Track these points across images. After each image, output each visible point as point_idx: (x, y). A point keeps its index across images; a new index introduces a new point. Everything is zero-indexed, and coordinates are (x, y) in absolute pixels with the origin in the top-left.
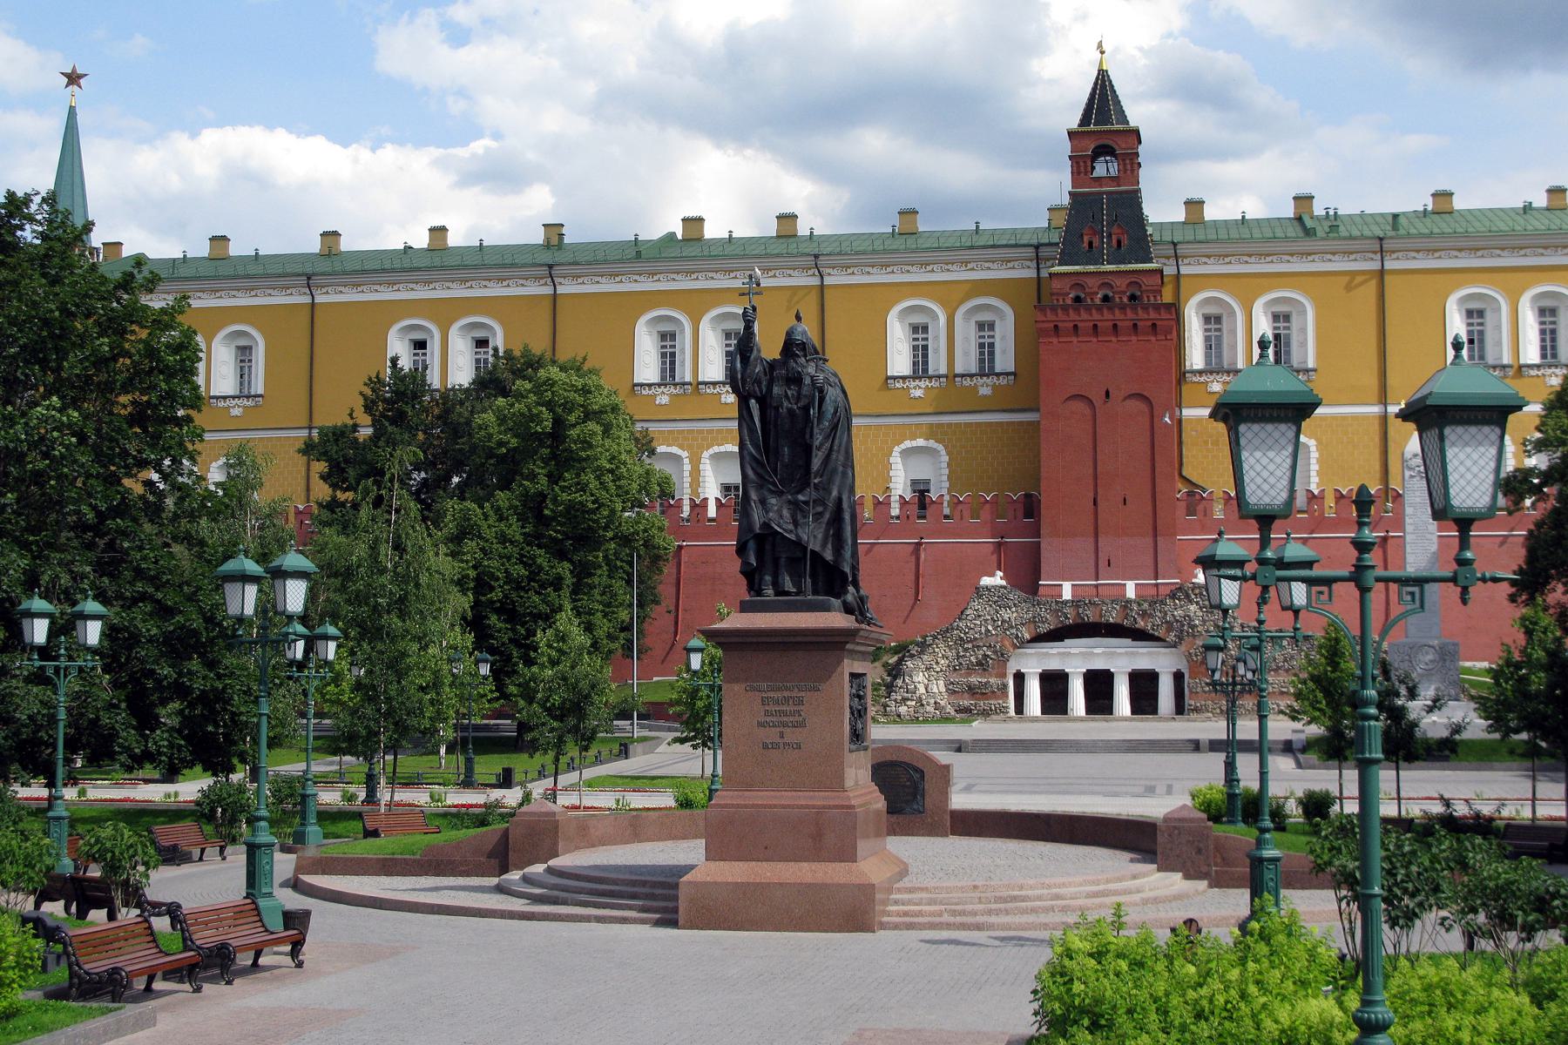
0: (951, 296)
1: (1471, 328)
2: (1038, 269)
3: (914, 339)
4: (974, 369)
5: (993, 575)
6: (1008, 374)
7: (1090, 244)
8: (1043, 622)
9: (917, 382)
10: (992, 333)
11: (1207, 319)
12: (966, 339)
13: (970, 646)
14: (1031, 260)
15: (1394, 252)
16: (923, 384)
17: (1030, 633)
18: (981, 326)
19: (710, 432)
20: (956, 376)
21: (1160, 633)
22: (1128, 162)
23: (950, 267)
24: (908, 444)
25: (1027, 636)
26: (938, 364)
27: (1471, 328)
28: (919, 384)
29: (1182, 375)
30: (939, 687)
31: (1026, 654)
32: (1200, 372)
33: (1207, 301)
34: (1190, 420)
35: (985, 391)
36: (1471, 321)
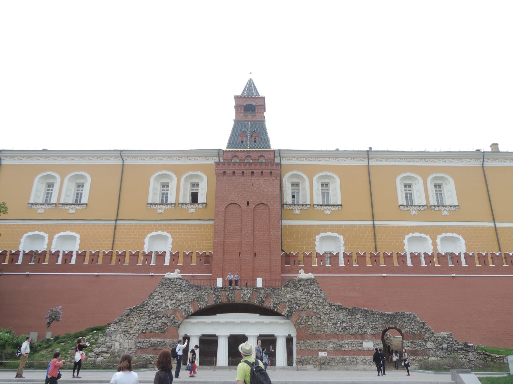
0: (178, 170)
1: (406, 192)
3: (163, 190)
5: (173, 272)
6: (203, 204)
7: (242, 142)
9: (161, 206)
11: (293, 185)
12: (185, 189)
13: (154, 316)
14: (216, 157)
15: (372, 158)
16: (163, 207)
17: (194, 309)
18: (193, 185)
19: (60, 226)
20: (179, 204)
22: (260, 109)
24: (154, 233)
25: (192, 311)
26: (171, 199)
27: (406, 192)
29: (282, 205)
31: (191, 322)
32: (290, 205)
33: (293, 176)
34: (285, 226)
35: (191, 211)
36: (406, 189)
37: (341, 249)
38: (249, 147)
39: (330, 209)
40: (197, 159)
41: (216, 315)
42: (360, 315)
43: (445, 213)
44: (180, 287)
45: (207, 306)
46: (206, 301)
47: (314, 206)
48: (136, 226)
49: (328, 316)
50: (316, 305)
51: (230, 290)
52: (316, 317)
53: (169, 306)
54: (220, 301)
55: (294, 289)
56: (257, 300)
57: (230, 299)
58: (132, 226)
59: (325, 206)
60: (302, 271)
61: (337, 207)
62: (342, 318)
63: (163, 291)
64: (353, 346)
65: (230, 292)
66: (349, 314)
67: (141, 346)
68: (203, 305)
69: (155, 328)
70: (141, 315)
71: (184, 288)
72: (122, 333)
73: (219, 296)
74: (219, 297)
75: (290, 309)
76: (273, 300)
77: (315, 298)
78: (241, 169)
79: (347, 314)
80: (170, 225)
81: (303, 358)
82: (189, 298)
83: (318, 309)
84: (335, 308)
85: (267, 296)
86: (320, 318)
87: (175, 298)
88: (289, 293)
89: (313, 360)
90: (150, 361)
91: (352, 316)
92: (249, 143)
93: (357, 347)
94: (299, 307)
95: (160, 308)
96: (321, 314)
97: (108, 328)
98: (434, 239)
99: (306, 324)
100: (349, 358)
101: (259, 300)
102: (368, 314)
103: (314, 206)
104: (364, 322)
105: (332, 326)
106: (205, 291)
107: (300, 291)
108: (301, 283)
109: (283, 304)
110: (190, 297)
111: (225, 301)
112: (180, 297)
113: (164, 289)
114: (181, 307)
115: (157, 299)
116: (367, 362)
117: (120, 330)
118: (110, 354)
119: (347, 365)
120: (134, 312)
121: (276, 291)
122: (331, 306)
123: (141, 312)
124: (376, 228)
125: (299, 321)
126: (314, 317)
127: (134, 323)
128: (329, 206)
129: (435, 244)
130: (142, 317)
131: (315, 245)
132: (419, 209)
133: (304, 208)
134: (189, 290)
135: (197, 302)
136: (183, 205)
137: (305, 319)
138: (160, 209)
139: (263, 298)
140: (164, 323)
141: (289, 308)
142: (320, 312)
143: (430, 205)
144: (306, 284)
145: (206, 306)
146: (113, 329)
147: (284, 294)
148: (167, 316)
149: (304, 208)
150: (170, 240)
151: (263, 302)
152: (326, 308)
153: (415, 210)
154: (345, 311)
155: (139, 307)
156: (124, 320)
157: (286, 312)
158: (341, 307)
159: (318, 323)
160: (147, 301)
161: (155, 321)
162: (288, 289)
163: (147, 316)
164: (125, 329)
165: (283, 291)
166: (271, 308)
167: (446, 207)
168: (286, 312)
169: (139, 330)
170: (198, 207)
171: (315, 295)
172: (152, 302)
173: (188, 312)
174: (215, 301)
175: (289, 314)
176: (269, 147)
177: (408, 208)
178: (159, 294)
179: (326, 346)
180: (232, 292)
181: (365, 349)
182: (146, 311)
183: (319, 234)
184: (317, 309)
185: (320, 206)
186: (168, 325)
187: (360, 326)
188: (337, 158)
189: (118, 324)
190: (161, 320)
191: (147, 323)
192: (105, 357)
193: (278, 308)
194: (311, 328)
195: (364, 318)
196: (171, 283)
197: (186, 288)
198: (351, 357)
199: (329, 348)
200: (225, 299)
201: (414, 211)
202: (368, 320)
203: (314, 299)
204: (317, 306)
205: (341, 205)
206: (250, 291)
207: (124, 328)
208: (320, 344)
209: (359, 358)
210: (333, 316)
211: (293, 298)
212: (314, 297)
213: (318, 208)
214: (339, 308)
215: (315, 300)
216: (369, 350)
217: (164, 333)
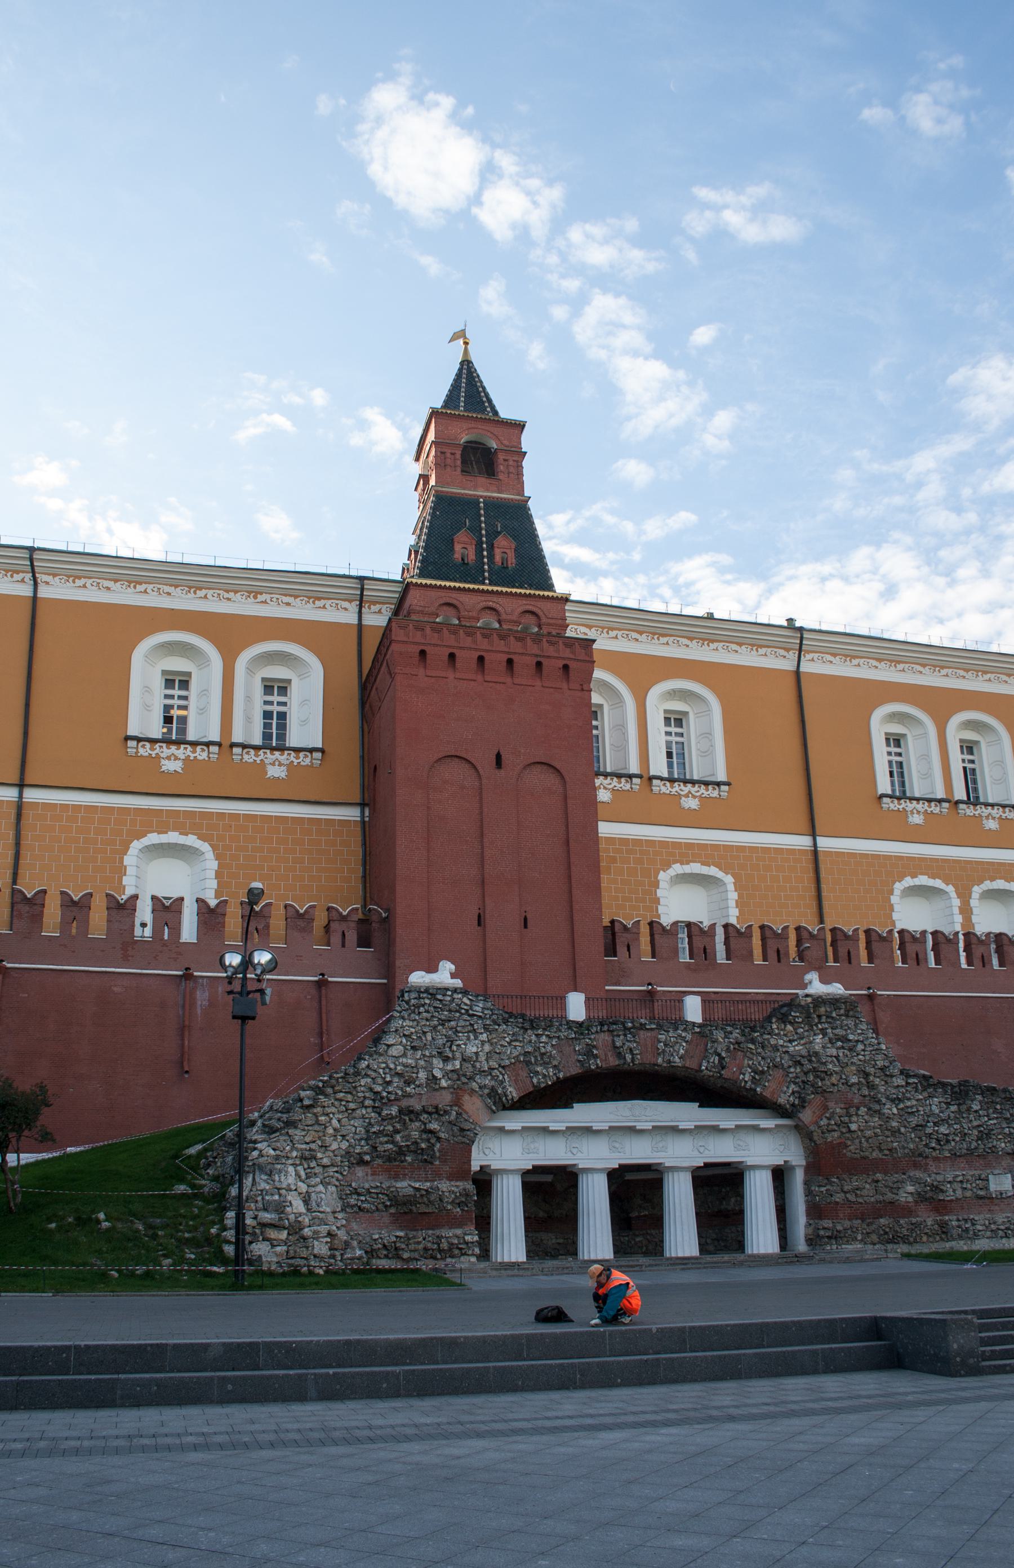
2: (360, 613)
4: (258, 741)
5: (432, 969)
6: (311, 750)
8: (545, 1064)
9: (173, 748)
10: (282, 699)
12: (248, 699)
14: (350, 601)
15: (809, 652)
16: (182, 752)
17: (517, 1089)
20: (233, 745)
21: (767, 1089)
23: (231, 595)
24: (153, 838)
25: (513, 1093)
27: (891, 758)
28: (176, 752)
30: (327, 1198)
31: (502, 1130)
35: (276, 772)
37: (730, 914)
38: (487, 581)
39: (698, 794)
40: (288, 604)
41: (572, 1107)
42: (980, 1102)
43: (992, 825)
44: (466, 1017)
45: (558, 1078)
46: (555, 1063)
47: (655, 782)
48: (91, 809)
49: (901, 1106)
50: (867, 1075)
51: (625, 1028)
52: (869, 1109)
53: (440, 1079)
54: (597, 1064)
55: (807, 1028)
56: (708, 1062)
57: (629, 1057)
58: (77, 808)
59: (682, 784)
60: (813, 977)
61: (714, 789)
62: (937, 1111)
63: (413, 1030)
64: (966, 1188)
65: (625, 1035)
66: (952, 1100)
67: (364, 1205)
68: (544, 1076)
69: (400, 1147)
70: (352, 1106)
71: (480, 1022)
72: (301, 1164)
73: (594, 1047)
74: (595, 1052)
75: (800, 1086)
76: (751, 1062)
77: (864, 1055)
78: (476, 650)
79: (947, 1098)
80: (204, 815)
81: (839, 1227)
82: (500, 1053)
83: (873, 1086)
84: (916, 1083)
85: (734, 1048)
86: (879, 1112)
87: (458, 1055)
88: (794, 1041)
89: (864, 1231)
90: (396, 1249)
91: (959, 1105)
92: (486, 567)
93: (975, 1190)
94: (822, 1080)
95: (413, 1086)
96: (884, 1100)
97: (255, 1149)
98: (964, 896)
99: (844, 1130)
100: (958, 1220)
101: (711, 1061)
102: (998, 1100)
103: (655, 782)
104: (992, 1122)
105: (913, 1136)
106: (546, 1033)
107: (821, 1036)
108: (822, 1010)
109: (779, 1073)
110: (504, 1049)
111: (613, 1061)
112: (472, 1049)
113: (415, 1023)
114: (479, 1081)
115: (399, 1057)
116: (999, 1229)
117: (294, 1154)
118: (286, 1232)
119: (954, 1239)
120: (326, 1096)
121: (756, 1034)
122: (908, 1076)
123: (349, 1097)
124: (821, 858)
125: (824, 1122)
126: (863, 1110)
127: (330, 1131)
128: (693, 782)
129: (966, 911)
130: (354, 1114)
131: (657, 901)
132: (929, 810)
133: (624, 785)
134: (497, 1027)
135: (528, 1065)
136: (245, 750)
137: (839, 1117)
138: (168, 758)
139: (724, 1054)
140: (431, 1132)
141: (795, 1083)
142: (880, 1095)
143: (956, 799)
144: (834, 1015)
145: (555, 1078)
146: (272, 1152)
147: (781, 1042)
148: (434, 1110)
149: (621, 785)
150: (212, 864)
151: (723, 1068)
152: (896, 1084)
153: (918, 812)
154: (941, 1090)
155: (340, 1080)
156: (300, 1120)
157: (789, 1096)
158: (931, 1080)
159: (874, 1128)
160: (366, 1063)
161: (398, 1126)
162: (789, 1027)
163: (370, 1110)
164: (306, 1150)
165: (776, 1035)
166: (745, 1086)
167: (993, 809)
168: (789, 1096)
169: (348, 1153)
170: (296, 762)
171: (865, 1045)
172: (384, 1065)
173: (500, 1098)
174: (583, 1065)
175: (797, 1102)
176: (550, 587)
177: (900, 804)
178: (404, 1041)
179: (895, 1191)
180: (634, 1037)
181: (994, 1196)
182: (367, 1095)
183: (669, 866)
184: (871, 1086)
185: (668, 784)
186: (439, 1139)
187: (981, 1131)
188: (713, 641)
189: (281, 1135)
190: (418, 1124)
191: (374, 1133)
192: (275, 1240)
193: (767, 1084)
194: (857, 1141)
195: (991, 1111)
196: (437, 1004)
197: (488, 1023)
198: (961, 1218)
199: (905, 1195)
200: (611, 1059)
201: (915, 815)
202: (999, 1115)
203: (860, 1057)
204: (871, 1078)
205: (728, 784)
206: (684, 1034)
207: (304, 1146)
208: (880, 1184)
209: (981, 1218)
210: (912, 1107)
211: (806, 1054)
212: (862, 1053)
213: (664, 790)
214: (927, 1083)
215: (865, 1061)
216: (1004, 1196)
217: (431, 1163)
